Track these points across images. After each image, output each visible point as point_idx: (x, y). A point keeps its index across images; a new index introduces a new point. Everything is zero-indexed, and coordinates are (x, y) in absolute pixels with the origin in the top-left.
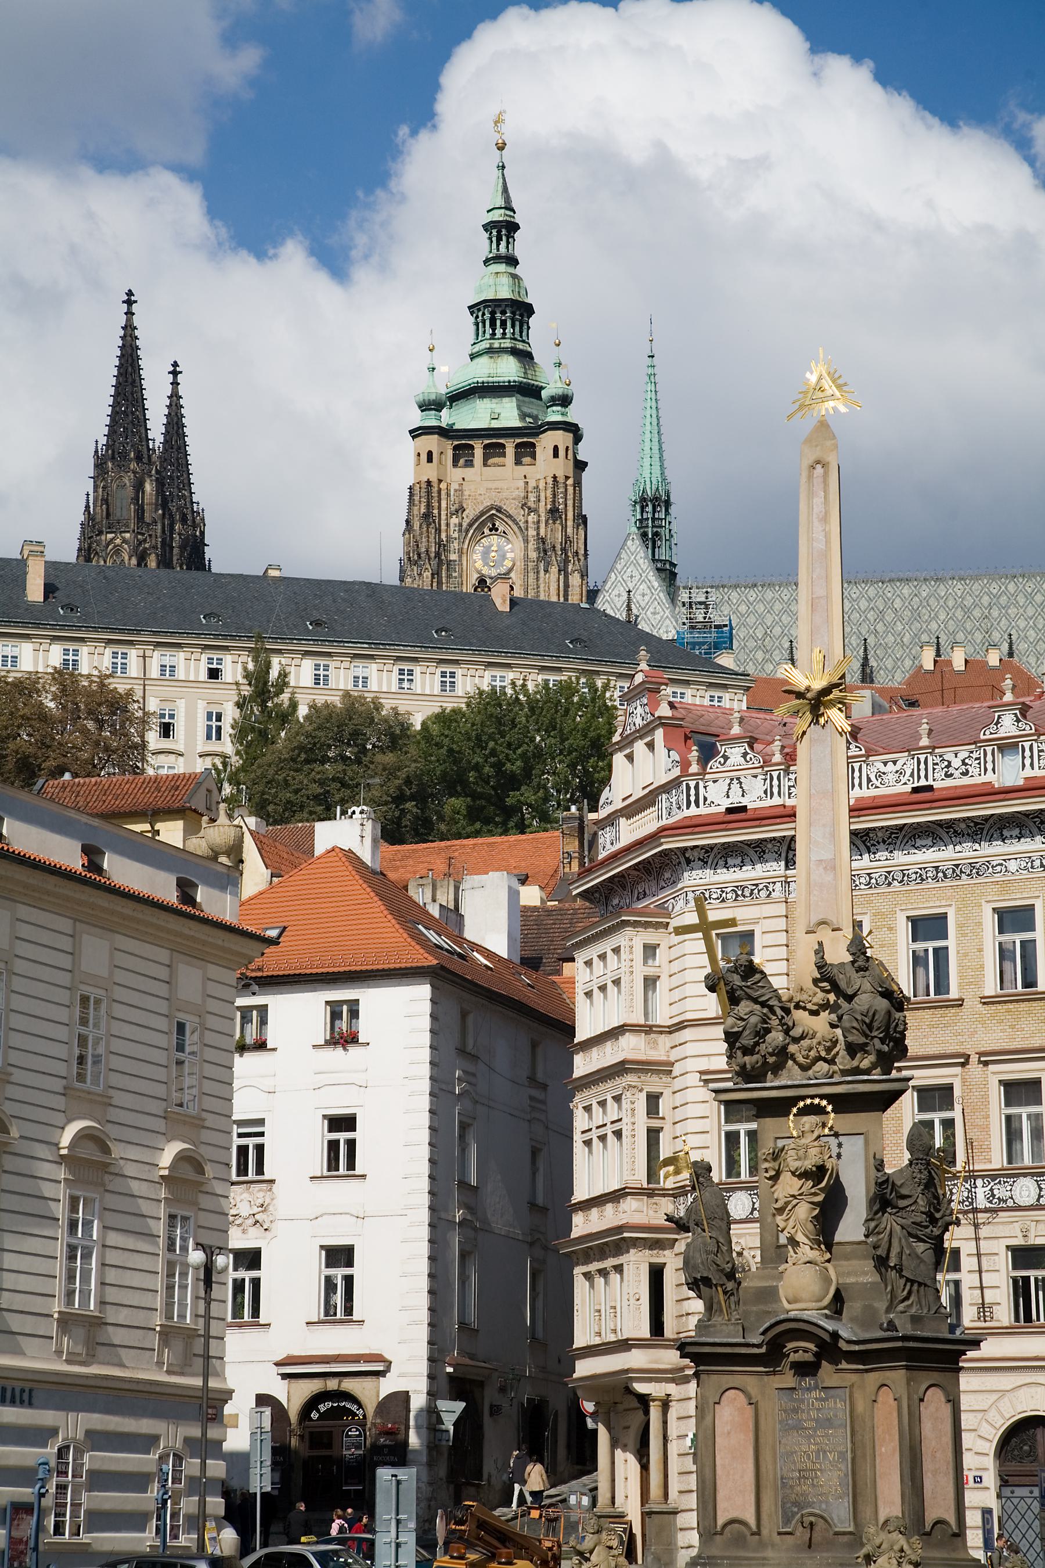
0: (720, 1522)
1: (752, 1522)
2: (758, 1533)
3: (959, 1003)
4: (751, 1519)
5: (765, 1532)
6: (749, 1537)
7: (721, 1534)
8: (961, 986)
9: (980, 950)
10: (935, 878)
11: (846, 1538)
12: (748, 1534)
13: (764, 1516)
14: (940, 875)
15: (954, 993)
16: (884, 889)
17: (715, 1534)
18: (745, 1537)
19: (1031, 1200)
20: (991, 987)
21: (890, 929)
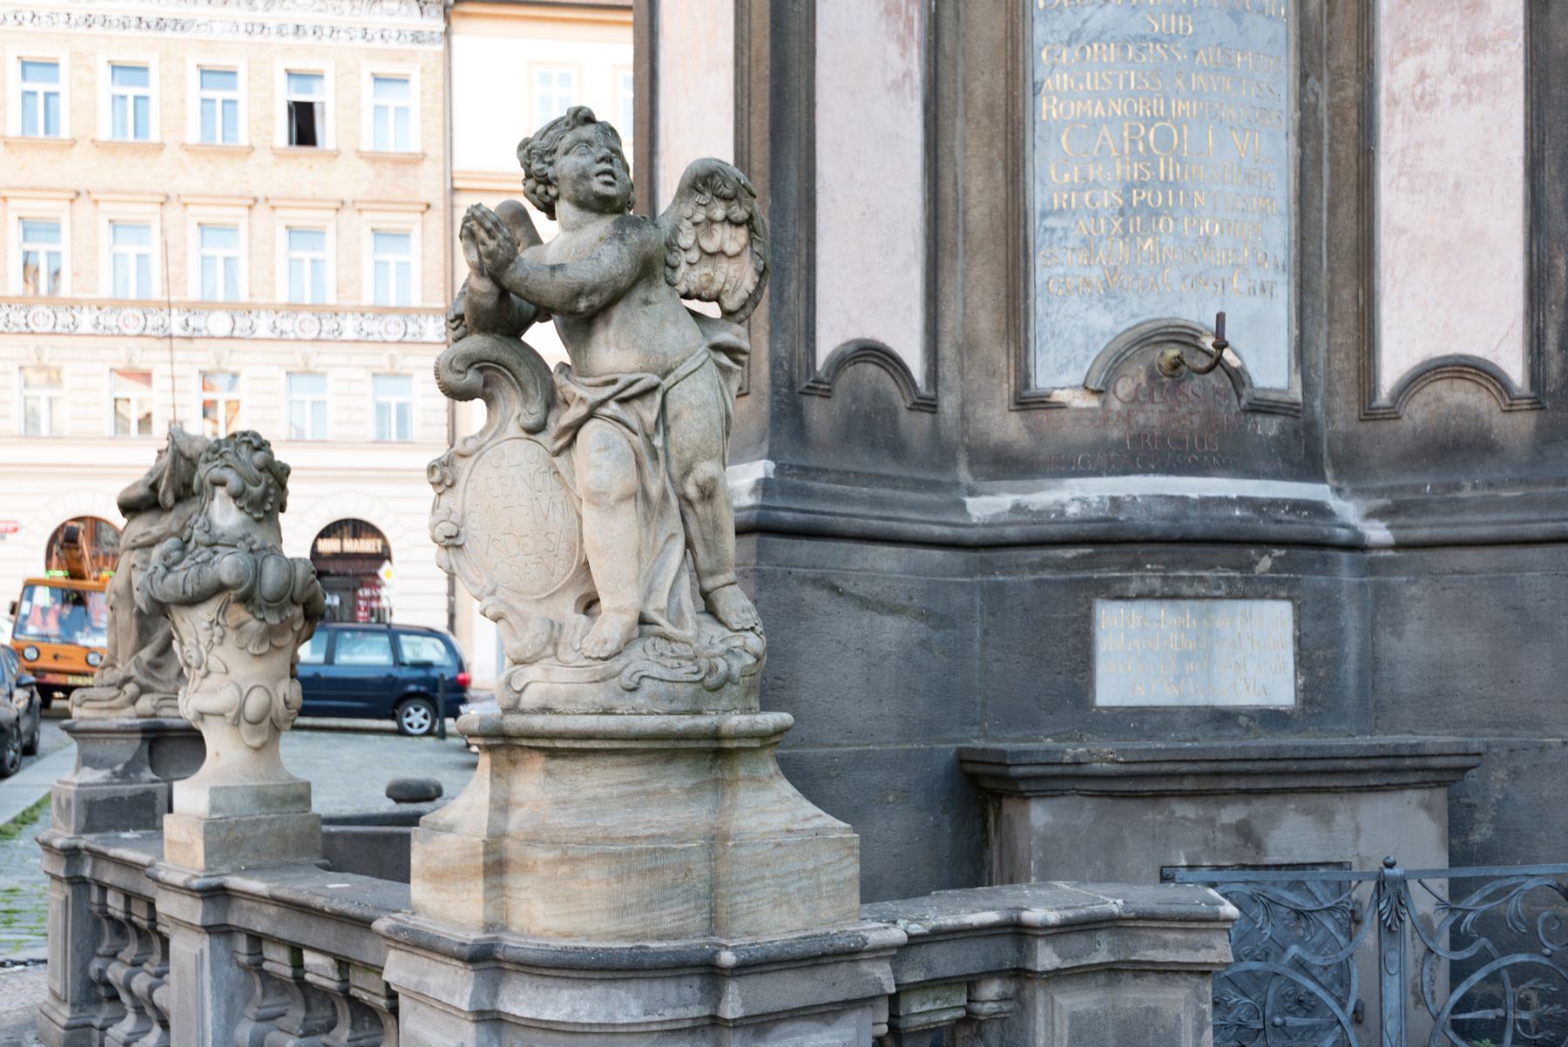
0: (827, 344)
1: (916, 364)
2: (929, 405)
3: (161, 147)
4: (914, 359)
5: (949, 403)
6: (904, 417)
7: (827, 395)
8: (162, 133)
9: (183, 101)
10: (138, 27)
11: (1270, 427)
12: (902, 403)
13: (947, 350)
14: (144, 25)
15: (155, 137)
16: (83, 29)
17: (810, 391)
18: (893, 413)
19: (226, 331)
20: (193, 136)
21: (90, 69)
